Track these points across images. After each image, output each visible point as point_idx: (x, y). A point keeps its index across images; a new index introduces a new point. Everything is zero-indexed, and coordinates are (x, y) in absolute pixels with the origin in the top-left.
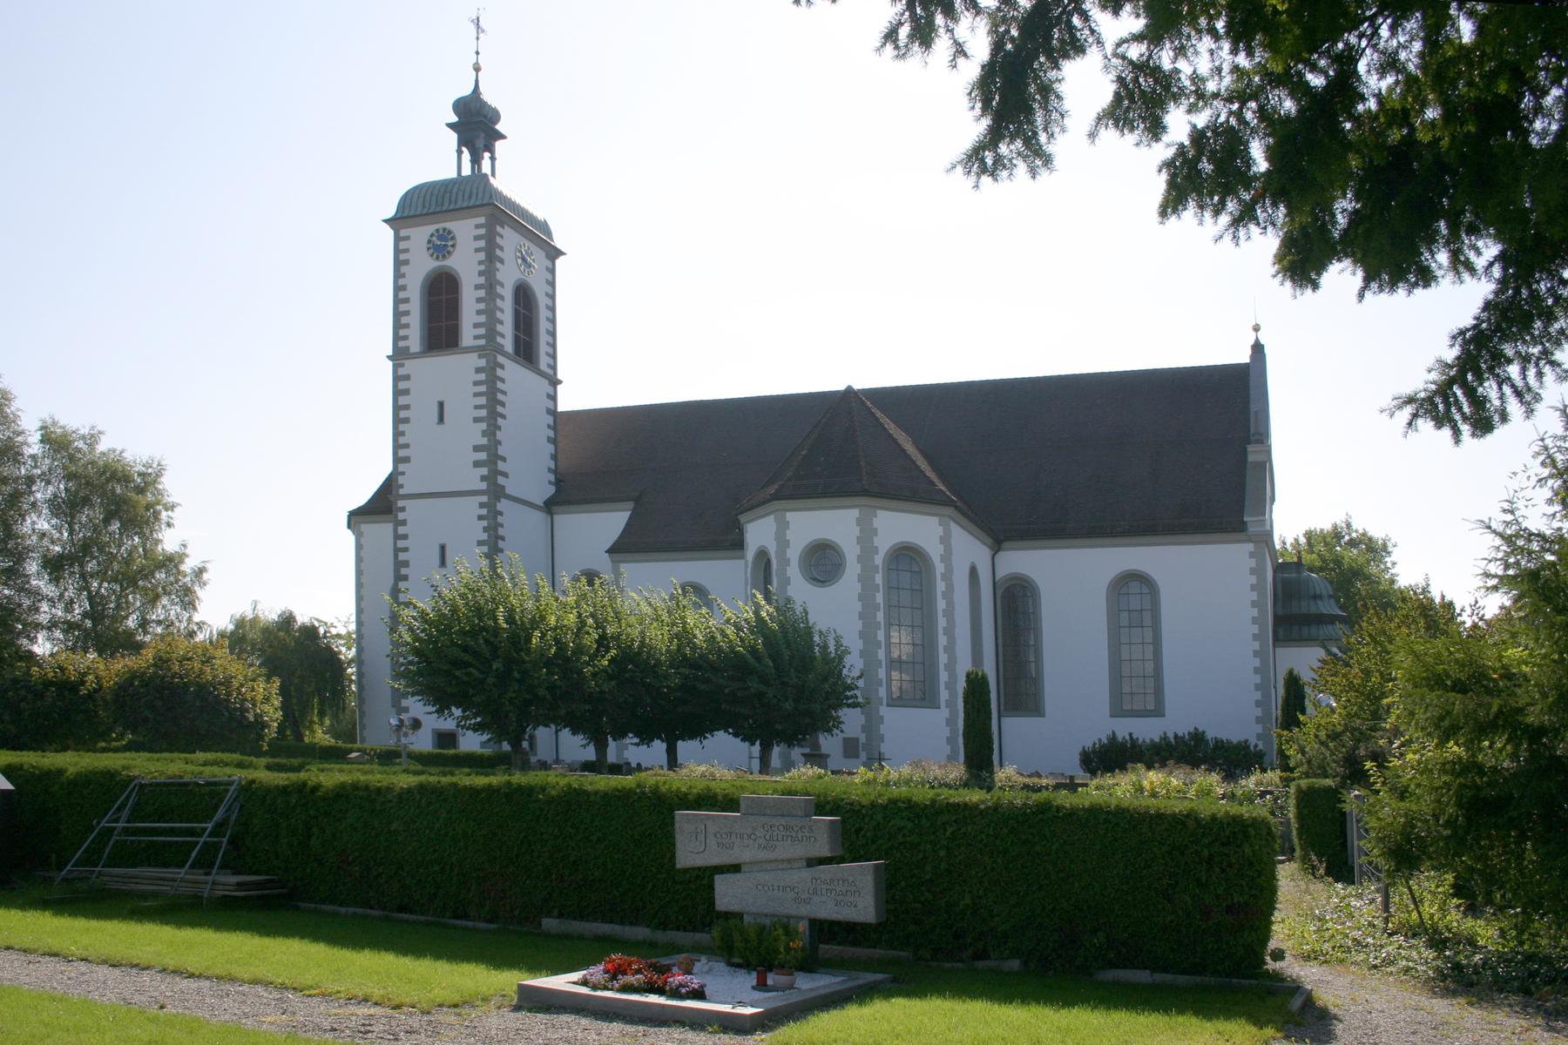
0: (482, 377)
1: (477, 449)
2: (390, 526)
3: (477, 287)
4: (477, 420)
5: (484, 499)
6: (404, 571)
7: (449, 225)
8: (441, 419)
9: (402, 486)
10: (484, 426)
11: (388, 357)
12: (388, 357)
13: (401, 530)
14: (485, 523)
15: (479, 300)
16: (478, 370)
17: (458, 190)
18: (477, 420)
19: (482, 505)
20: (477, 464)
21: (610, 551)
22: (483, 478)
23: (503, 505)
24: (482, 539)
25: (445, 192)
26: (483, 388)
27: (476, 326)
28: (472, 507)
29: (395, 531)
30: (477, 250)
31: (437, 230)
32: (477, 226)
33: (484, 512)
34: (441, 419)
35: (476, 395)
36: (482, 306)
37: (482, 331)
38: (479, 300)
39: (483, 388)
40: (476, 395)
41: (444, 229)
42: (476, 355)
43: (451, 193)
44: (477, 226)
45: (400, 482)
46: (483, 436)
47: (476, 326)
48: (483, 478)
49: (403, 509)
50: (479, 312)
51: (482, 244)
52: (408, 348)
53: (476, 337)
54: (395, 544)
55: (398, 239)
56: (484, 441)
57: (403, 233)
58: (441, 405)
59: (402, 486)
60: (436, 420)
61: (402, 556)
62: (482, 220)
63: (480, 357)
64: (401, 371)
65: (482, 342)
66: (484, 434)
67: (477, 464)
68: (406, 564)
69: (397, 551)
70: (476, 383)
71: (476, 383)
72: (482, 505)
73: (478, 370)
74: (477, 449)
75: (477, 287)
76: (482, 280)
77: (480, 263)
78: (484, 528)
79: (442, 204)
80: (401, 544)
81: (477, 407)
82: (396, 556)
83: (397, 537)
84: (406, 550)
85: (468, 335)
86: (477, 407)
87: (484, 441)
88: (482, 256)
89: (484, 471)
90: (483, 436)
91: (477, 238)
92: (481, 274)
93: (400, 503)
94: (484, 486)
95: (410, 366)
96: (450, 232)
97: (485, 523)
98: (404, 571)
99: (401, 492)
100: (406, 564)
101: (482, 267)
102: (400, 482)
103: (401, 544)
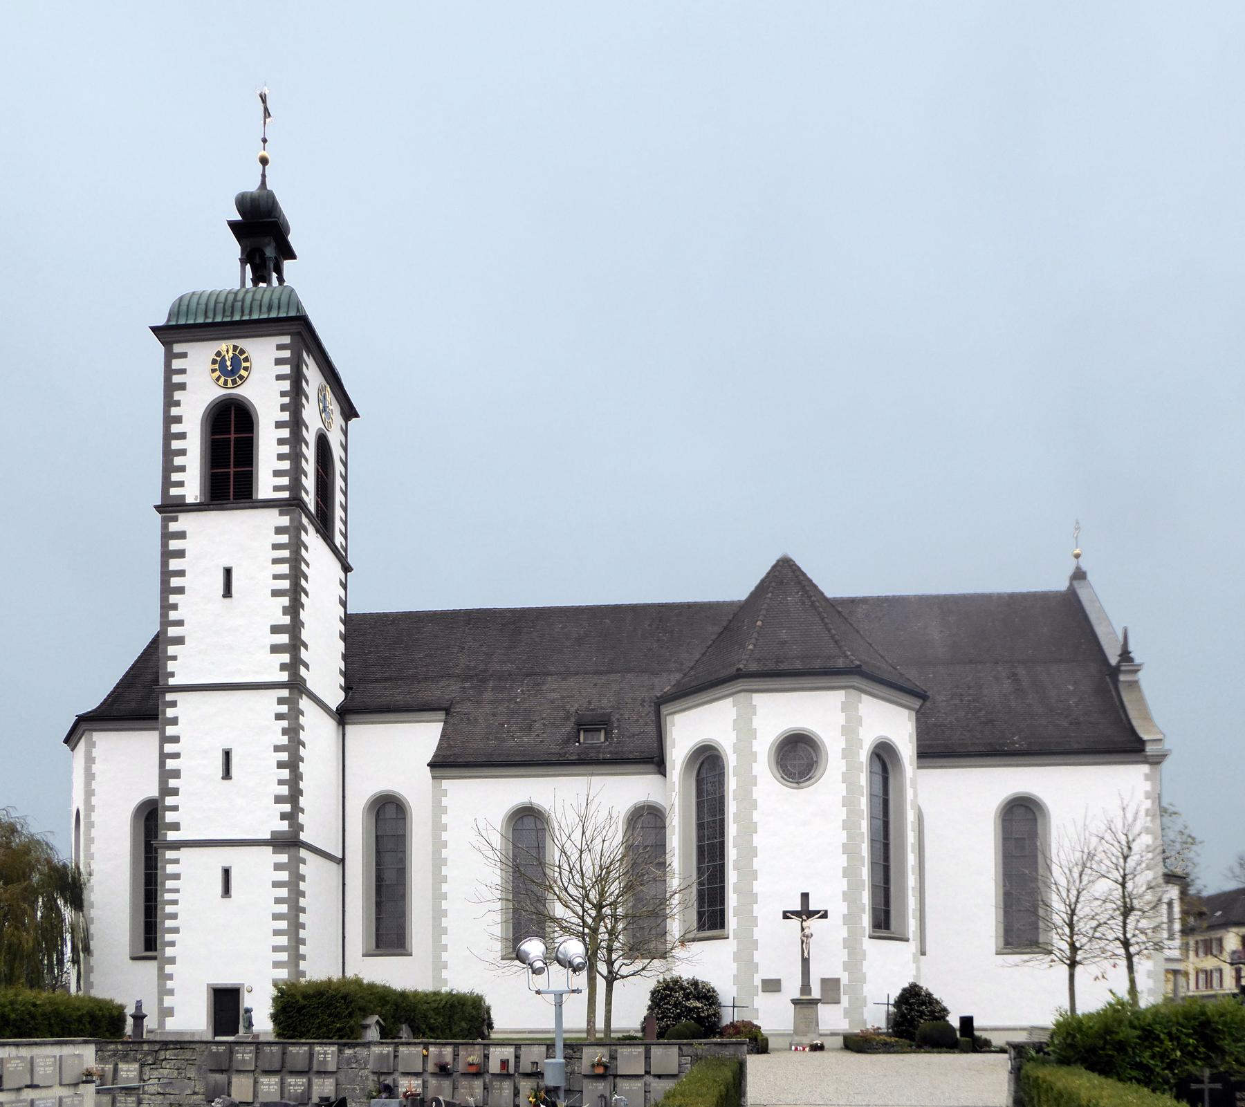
0: (285, 539)
1: (275, 629)
3: (279, 425)
4: (276, 593)
5: (285, 693)
6: (172, 783)
8: (228, 593)
9: (172, 675)
10: (285, 601)
11: (156, 507)
12: (156, 507)
14: (285, 723)
15: (281, 442)
18: (276, 593)
19: (281, 701)
20: (275, 649)
21: (432, 765)
22: (283, 667)
23: (305, 703)
24: (279, 743)
25: (235, 300)
26: (285, 553)
27: (277, 473)
28: (269, 703)
30: (279, 378)
33: (284, 709)
34: (228, 593)
35: (276, 561)
36: (286, 449)
37: (285, 481)
38: (281, 442)
39: (285, 553)
40: (276, 561)
42: (275, 512)
44: (280, 347)
45: (169, 670)
47: (277, 473)
48: (283, 667)
49: (173, 704)
50: (281, 457)
51: (286, 369)
52: (183, 497)
53: (277, 489)
54: (161, 748)
55: (170, 356)
56: (286, 620)
57: (178, 348)
58: (228, 572)
59: (172, 675)
61: (171, 764)
62: (286, 340)
63: (281, 514)
64: (173, 527)
65: (285, 495)
66: (286, 611)
67: (275, 649)
68: (176, 774)
69: (163, 757)
70: (276, 547)
71: (276, 547)
72: (281, 701)
73: (279, 531)
74: (275, 629)
75: (279, 425)
76: (286, 416)
77: (283, 394)
78: (283, 729)
79: (232, 314)
80: (169, 748)
81: (276, 577)
82: (162, 764)
84: (176, 756)
85: (267, 484)
86: (276, 577)
87: (286, 620)
88: (286, 385)
89: (285, 658)
91: (279, 362)
92: (283, 408)
93: (169, 697)
94: (284, 677)
95: (184, 522)
96: (242, 352)
97: (285, 723)
98: (172, 783)
99: (172, 681)
100: (176, 774)
101: (286, 400)
102: (169, 670)
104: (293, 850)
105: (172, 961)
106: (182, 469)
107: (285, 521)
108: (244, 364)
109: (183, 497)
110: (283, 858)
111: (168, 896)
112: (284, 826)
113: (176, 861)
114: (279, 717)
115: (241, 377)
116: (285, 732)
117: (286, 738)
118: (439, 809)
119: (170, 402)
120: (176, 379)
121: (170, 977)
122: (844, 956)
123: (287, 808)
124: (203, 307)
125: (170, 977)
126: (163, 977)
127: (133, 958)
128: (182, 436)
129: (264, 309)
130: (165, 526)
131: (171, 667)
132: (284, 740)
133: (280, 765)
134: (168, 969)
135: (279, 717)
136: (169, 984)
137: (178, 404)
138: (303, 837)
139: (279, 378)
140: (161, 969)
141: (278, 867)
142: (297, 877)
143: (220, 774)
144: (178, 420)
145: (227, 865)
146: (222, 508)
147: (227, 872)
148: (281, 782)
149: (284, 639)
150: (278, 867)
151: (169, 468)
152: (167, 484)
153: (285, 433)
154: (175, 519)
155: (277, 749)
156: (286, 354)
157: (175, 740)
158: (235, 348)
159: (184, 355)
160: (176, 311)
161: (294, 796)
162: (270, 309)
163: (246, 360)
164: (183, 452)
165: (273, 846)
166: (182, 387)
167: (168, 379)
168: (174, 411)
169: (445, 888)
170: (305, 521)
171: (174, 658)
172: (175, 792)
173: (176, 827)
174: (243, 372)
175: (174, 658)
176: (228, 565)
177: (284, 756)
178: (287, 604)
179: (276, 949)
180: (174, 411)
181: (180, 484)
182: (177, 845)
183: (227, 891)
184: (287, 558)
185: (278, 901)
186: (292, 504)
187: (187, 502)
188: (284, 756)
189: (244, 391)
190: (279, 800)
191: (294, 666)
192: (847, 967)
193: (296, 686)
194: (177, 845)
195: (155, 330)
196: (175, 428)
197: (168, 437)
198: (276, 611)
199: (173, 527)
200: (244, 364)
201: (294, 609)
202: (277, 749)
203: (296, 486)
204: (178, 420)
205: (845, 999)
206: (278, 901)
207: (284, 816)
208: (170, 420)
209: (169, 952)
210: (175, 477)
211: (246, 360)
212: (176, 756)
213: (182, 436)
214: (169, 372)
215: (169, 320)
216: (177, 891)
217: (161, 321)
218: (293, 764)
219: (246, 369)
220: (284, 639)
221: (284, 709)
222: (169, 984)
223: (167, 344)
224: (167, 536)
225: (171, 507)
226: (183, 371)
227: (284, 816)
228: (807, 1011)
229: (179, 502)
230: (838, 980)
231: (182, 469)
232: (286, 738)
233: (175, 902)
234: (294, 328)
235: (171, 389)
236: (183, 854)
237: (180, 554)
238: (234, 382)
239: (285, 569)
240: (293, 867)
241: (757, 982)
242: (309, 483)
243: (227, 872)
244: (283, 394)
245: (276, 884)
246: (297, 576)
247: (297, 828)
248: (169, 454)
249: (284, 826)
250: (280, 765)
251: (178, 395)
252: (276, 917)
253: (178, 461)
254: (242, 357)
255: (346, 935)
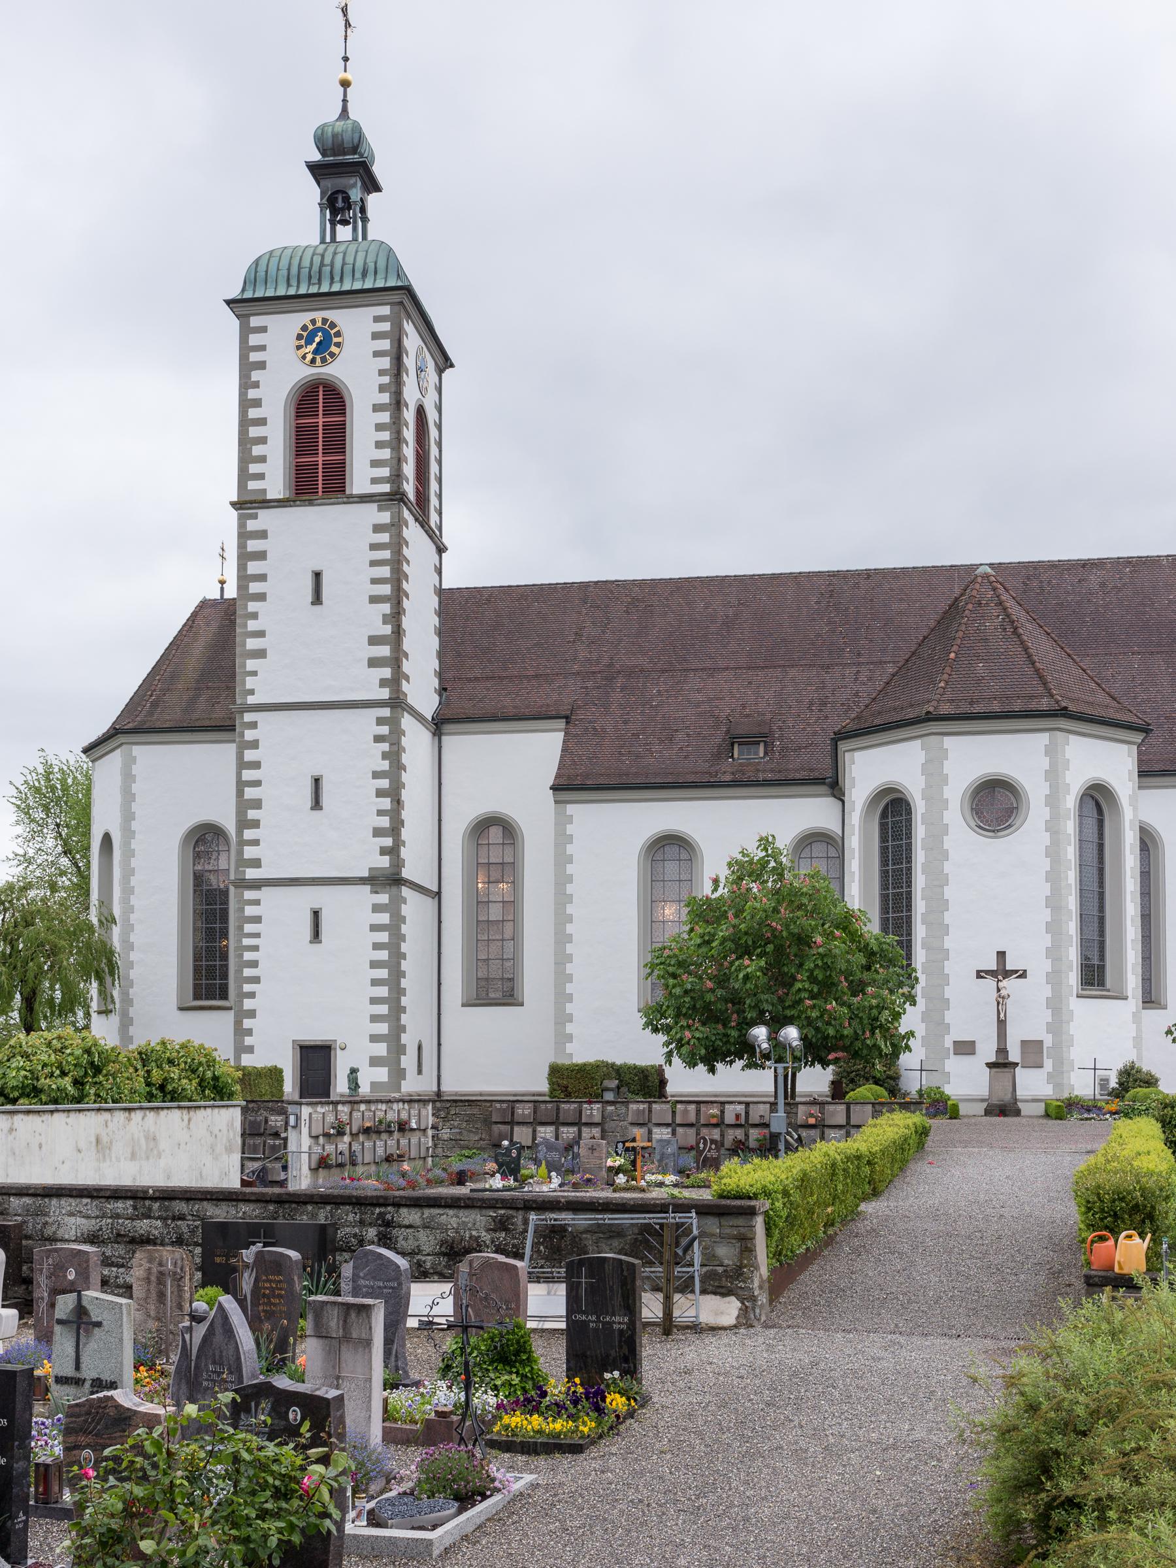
0: (385, 538)
1: (374, 640)
2: (230, 750)
3: (377, 408)
4: (374, 599)
5: (386, 712)
6: (252, 814)
7: (332, 315)
8: (317, 599)
9: (252, 692)
10: (386, 608)
11: (233, 504)
12: (233, 504)
13: (249, 755)
14: (385, 747)
15: (379, 427)
16: (378, 528)
17: (344, 264)
18: (374, 599)
20: (373, 663)
22: (383, 683)
24: (379, 769)
25: (322, 264)
26: (386, 554)
27: (375, 464)
28: (366, 723)
29: (240, 756)
30: (377, 354)
31: (313, 322)
32: (377, 319)
33: (384, 730)
34: (317, 599)
35: (373, 563)
36: (385, 436)
38: (379, 427)
39: (386, 554)
40: (373, 563)
41: (325, 321)
42: (374, 506)
43: (332, 265)
44: (377, 319)
46: (384, 623)
47: (375, 464)
48: (383, 683)
50: (379, 445)
51: (385, 345)
52: (264, 491)
53: (374, 481)
54: (239, 775)
55: (246, 331)
57: (255, 321)
58: (317, 575)
59: (252, 692)
60: (309, 596)
61: (250, 793)
62: (385, 310)
63: (380, 509)
64: (252, 525)
65: (386, 488)
66: (386, 619)
67: (373, 663)
68: (257, 804)
69: (241, 785)
70: (374, 547)
71: (374, 547)
72: (380, 721)
73: (378, 528)
74: (374, 640)
75: (377, 408)
77: (382, 373)
79: (320, 283)
80: (248, 775)
81: (374, 581)
82: (240, 793)
83: (242, 765)
85: (361, 477)
86: (374, 581)
88: (385, 363)
89: (387, 673)
90: (384, 623)
91: (376, 336)
93: (248, 717)
94: (385, 694)
95: (264, 519)
96: (333, 325)
97: (385, 747)
98: (252, 814)
99: (251, 700)
100: (257, 804)
102: (248, 687)
103: (248, 775)
104: (394, 889)
105: (252, 1014)
106: (262, 459)
107: (385, 517)
108: (335, 340)
109: (264, 491)
110: (383, 898)
111: (246, 942)
112: (385, 862)
113: (257, 902)
114: (378, 739)
115: (332, 355)
116: (385, 756)
117: (387, 762)
118: (562, 839)
119: (246, 384)
120: (254, 357)
121: (249, 1032)
122: (1048, 1016)
123: (388, 842)
124: (284, 272)
125: (249, 1032)
126: (241, 1032)
127: (181, 1009)
128: (262, 422)
129: (358, 275)
130: (242, 525)
131: (250, 683)
132: (385, 765)
133: (380, 793)
134: (247, 1023)
135: (378, 739)
136: (248, 1041)
137: (256, 385)
138: (406, 873)
139: (377, 354)
140: (238, 1023)
141: (377, 908)
142: (398, 919)
143: (309, 803)
144: (257, 403)
145: (316, 906)
146: (311, 503)
147: (316, 914)
148: (380, 813)
149: (385, 651)
150: (377, 908)
151: (246, 458)
152: (244, 476)
153: (385, 417)
154: (255, 517)
155: (376, 775)
156: (386, 326)
157: (256, 765)
158: (325, 321)
159: (264, 329)
160: (251, 280)
161: (395, 829)
162: (364, 274)
163: (338, 334)
164: (263, 440)
165: (372, 885)
166: (261, 365)
167: (243, 357)
168: (252, 394)
169: (569, 929)
170: (406, 514)
171: (254, 673)
172: (256, 824)
173: (256, 863)
174: (333, 349)
175: (254, 673)
176: (317, 569)
177: (384, 783)
178: (388, 612)
179: (374, 1001)
180: (252, 394)
181: (261, 477)
182: (257, 884)
183: (316, 935)
184: (387, 560)
185: (377, 946)
186: (396, 497)
187: (268, 497)
188: (384, 783)
189: (333, 370)
190: (378, 832)
191: (395, 682)
192: (1050, 1028)
193: (397, 703)
194: (257, 884)
195: (229, 302)
196: (253, 413)
197: (245, 423)
198: (375, 620)
199: (252, 525)
200: (335, 340)
201: (396, 617)
202: (376, 775)
203: (397, 477)
204: (257, 403)
205: (1048, 1064)
206: (377, 946)
207: (384, 851)
208: (246, 404)
209: (248, 1004)
210: (254, 468)
211: (338, 334)
212: (257, 783)
213: (262, 422)
214: (245, 349)
215: (243, 290)
216: (257, 935)
217: (234, 292)
218: (394, 793)
219: (338, 345)
220: (385, 651)
221: (384, 730)
222: (248, 1041)
223: (243, 318)
224: (244, 536)
225: (248, 504)
226: (262, 348)
227: (384, 851)
228: (1004, 1074)
229: (260, 498)
230: (1040, 1043)
231: (262, 459)
232: (387, 762)
233: (255, 948)
234: (396, 297)
235: (248, 369)
236: (264, 894)
237: (261, 556)
238: (324, 360)
239: (385, 572)
240: (394, 909)
241: (948, 1043)
242: (409, 469)
243: (316, 914)
244: (382, 373)
245: (374, 928)
246: (398, 578)
247: (398, 863)
248: (245, 443)
249: (385, 862)
250: (380, 793)
251: (255, 376)
252: (374, 965)
253: (257, 450)
254: (332, 332)
255: (442, 981)
